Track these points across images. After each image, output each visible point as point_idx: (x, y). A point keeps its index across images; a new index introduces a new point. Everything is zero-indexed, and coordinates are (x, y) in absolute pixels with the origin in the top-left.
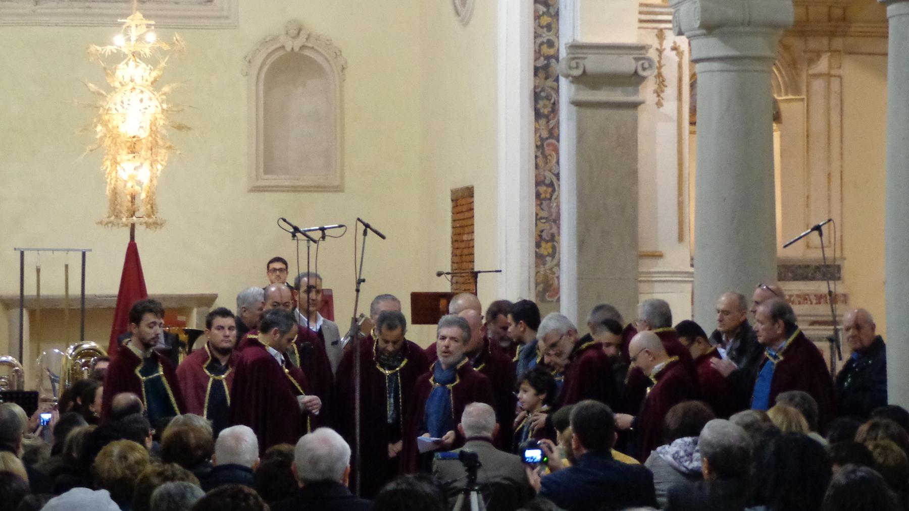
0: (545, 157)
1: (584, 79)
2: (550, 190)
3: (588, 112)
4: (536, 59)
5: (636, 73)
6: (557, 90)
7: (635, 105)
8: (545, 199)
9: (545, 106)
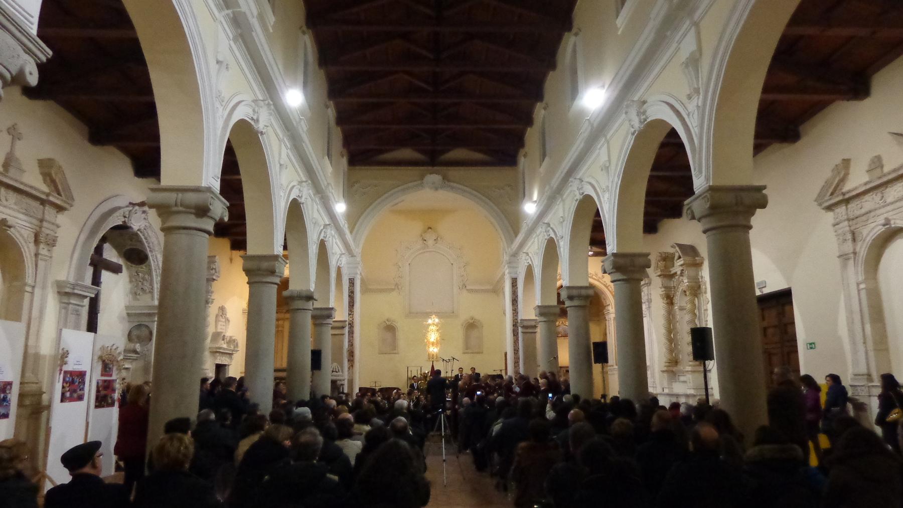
1: (524, 327)
5: (535, 326)
6: (518, 330)
7: (535, 333)
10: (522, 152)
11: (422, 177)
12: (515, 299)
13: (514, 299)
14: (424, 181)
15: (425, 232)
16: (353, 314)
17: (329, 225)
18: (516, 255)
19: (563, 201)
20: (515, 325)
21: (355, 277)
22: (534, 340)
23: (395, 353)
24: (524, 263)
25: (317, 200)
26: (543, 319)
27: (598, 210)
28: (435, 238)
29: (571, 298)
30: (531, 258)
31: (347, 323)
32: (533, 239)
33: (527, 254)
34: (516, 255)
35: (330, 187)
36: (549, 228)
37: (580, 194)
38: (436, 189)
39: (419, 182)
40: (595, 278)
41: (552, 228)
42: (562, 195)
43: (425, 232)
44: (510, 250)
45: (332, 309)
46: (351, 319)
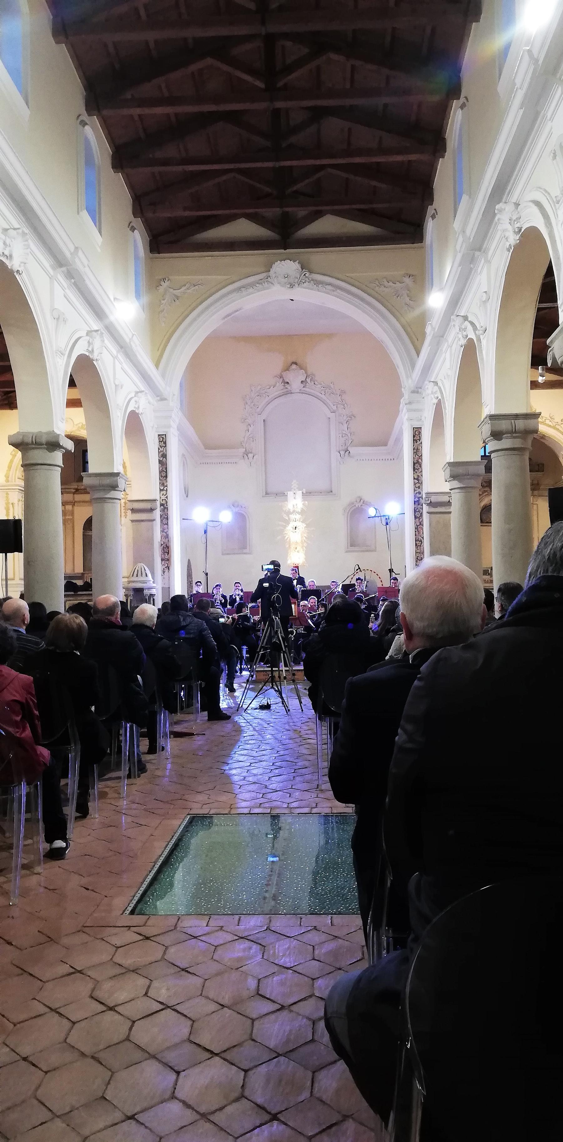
0: (418, 531)
1: (431, 504)
2: (420, 542)
3: (433, 515)
4: (415, 498)
6: (422, 509)
7: (450, 513)
8: (419, 546)
9: (418, 514)
10: (430, 210)
11: (268, 268)
12: (418, 462)
13: (415, 462)
14: (272, 273)
15: (287, 369)
16: (167, 490)
17: (97, 331)
18: (420, 390)
19: (488, 262)
20: (417, 502)
21: (167, 432)
22: (447, 526)
23: (245, 553)
24: (432, 399)
25: (61, 278)
26: (456, 484)
27: (551, 262)
28: (304, 379)
29: (496, 435)
30: (440, 388)
31: (158, 503)
32: (444, 355)
33: (436, 383)
34: (420, 390)
35: (80, 253)
36: (467, 323)
37: (514, 232)
38: (292, 286)
39: (264, 275)
40: (550, 423)
41: (472, 323)
42: (486, 252)
43: (287, 369)
44: (410, 381)
45: (118, 474)
46: (163, 497)
